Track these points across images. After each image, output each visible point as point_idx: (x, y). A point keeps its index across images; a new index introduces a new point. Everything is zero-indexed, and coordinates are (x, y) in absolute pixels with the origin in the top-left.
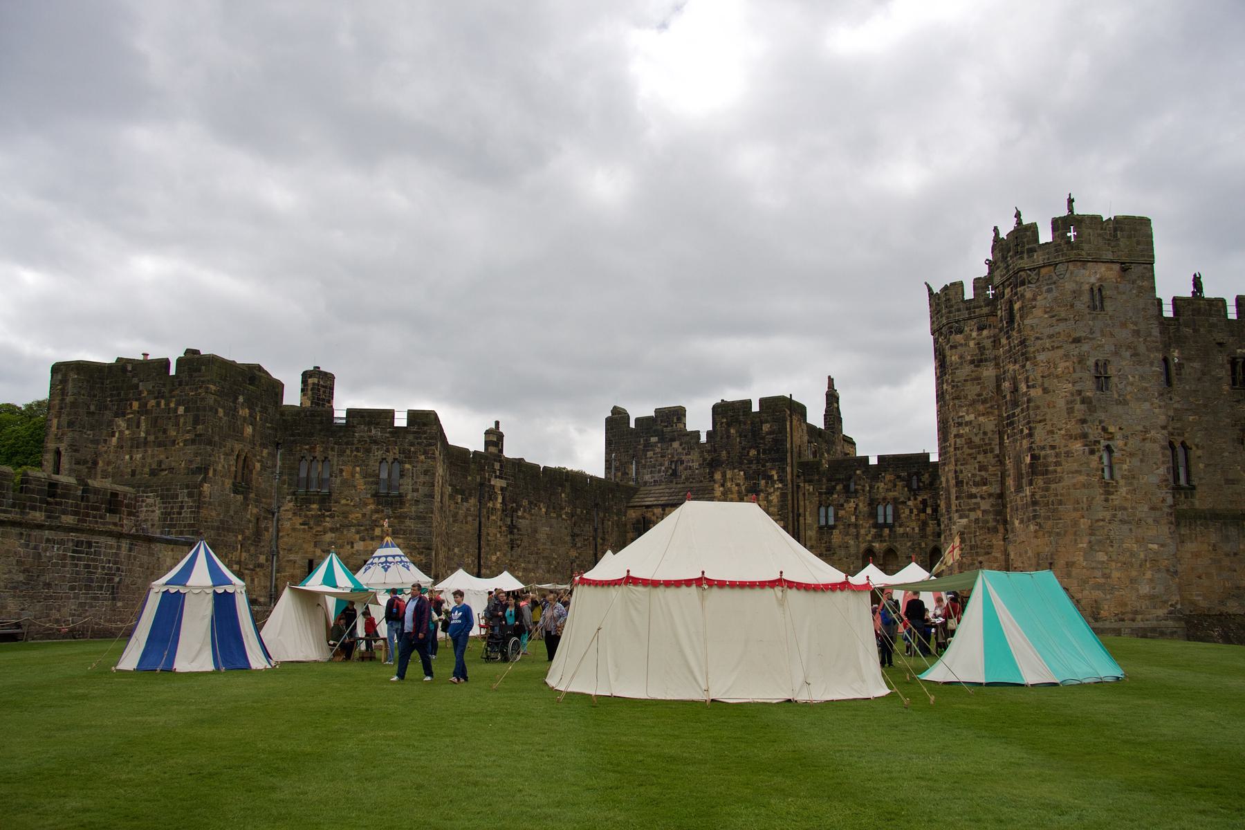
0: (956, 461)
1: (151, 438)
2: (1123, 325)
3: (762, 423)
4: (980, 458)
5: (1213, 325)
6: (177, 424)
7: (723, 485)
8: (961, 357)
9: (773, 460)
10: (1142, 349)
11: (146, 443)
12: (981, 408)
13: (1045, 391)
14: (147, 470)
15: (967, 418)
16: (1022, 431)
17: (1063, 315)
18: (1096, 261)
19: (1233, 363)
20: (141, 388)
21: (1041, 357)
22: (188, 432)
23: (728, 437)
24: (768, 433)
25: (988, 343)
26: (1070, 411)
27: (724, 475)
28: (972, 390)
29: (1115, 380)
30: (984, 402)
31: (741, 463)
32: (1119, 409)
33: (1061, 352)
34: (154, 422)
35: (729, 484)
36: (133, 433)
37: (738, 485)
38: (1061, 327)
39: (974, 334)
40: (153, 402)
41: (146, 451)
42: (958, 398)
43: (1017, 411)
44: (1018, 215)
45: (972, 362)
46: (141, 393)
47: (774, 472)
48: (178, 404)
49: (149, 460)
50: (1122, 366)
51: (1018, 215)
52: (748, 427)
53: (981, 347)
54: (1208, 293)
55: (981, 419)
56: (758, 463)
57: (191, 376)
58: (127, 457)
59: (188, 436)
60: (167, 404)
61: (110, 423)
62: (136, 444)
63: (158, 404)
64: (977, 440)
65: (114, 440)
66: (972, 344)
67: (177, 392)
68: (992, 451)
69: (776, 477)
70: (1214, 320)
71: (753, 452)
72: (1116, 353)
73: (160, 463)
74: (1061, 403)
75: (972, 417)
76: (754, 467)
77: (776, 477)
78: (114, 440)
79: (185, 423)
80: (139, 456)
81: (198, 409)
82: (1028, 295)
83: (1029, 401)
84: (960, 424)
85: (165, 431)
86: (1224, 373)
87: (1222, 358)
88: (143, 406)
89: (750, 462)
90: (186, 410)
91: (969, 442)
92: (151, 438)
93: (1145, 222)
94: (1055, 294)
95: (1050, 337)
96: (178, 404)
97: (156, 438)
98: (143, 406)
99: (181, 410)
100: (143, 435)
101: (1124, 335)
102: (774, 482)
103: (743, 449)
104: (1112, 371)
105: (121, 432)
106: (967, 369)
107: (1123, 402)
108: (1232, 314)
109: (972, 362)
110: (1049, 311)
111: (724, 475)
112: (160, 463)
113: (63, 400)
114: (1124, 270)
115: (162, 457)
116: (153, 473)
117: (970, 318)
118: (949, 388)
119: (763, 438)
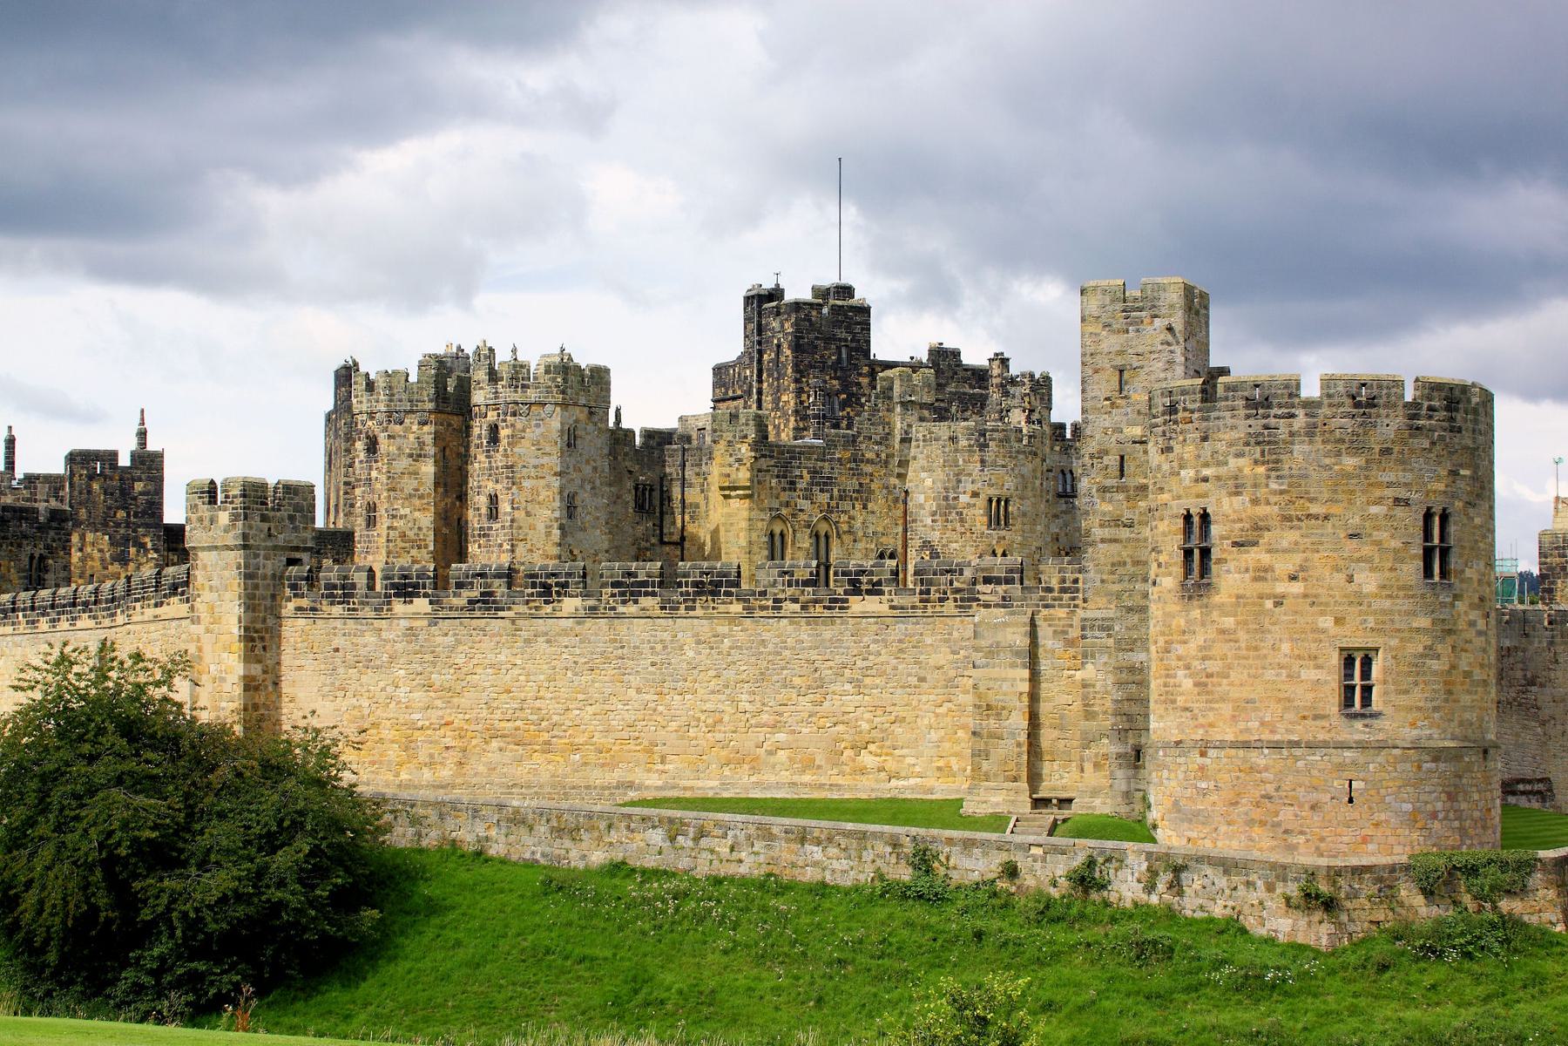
0: (389, 553)
2: (588, 462)
3: (134, 480)
4: (414, 552)
5: (626, 454)
7: (81, 550)
8: (399, 449)
9: (147, 526)
10: (598, 482)
12: (417, 502)
13: (528, 514)
15: (402, 512)
16: (501, 545)
17: (548, 449)
18: (575, 404)
19: (636, 489)
21: (526, 484)
23: (89, 492)
24: (141, 494)
25: (429, 439)
26: (548, 534)
27: (83, 537)
28: (409, 484)
29: (579, 509)
30: (421, 497)
31: (105, 525)
32: (580, 535)
33: (542, 482)
35: (89, 549)
37: (101, 551)
38: (545, 460)
39: (415, 428)
42: (393, 489)
43: (495, 526)
44: (514, 351)
45: (411, 456)
47: (147, 540)
50: (584, 496)
51: (514, 351)
52: (116, 483)
53: (422, 444)
54: (625, 425)
55: (417, 514)
56: (128, 526)
64: (411, 534)
66: (411, 437)
68: (426, 547)
69: (149, 545)
70: (627, 449)
71: (121, 514)
72: (582, 487)
74: (541, 527)
75: (407, 511)
76: (122, 531)
77: (149, 545)
82: (519, 426)
83: (512, 521)
84: (394, 517)
86: (629, 498)
87: (629, 484)
89: (118, 525)
91: (403, 535)
93: (607, 371)
94: (542, 429)
95: (535, 467)
101: (588, 470)
102: (146, 551)
103: (109, 508)
104: (578, 502)
106: (404, 463)
107: (583, 529)
108: (638, 441)
109: (411, 456)
110: (536, 443)
111: (83, 537)
114: (591, 413)
117: (412, 412)
118: (383, 478)
119: (135, 499)
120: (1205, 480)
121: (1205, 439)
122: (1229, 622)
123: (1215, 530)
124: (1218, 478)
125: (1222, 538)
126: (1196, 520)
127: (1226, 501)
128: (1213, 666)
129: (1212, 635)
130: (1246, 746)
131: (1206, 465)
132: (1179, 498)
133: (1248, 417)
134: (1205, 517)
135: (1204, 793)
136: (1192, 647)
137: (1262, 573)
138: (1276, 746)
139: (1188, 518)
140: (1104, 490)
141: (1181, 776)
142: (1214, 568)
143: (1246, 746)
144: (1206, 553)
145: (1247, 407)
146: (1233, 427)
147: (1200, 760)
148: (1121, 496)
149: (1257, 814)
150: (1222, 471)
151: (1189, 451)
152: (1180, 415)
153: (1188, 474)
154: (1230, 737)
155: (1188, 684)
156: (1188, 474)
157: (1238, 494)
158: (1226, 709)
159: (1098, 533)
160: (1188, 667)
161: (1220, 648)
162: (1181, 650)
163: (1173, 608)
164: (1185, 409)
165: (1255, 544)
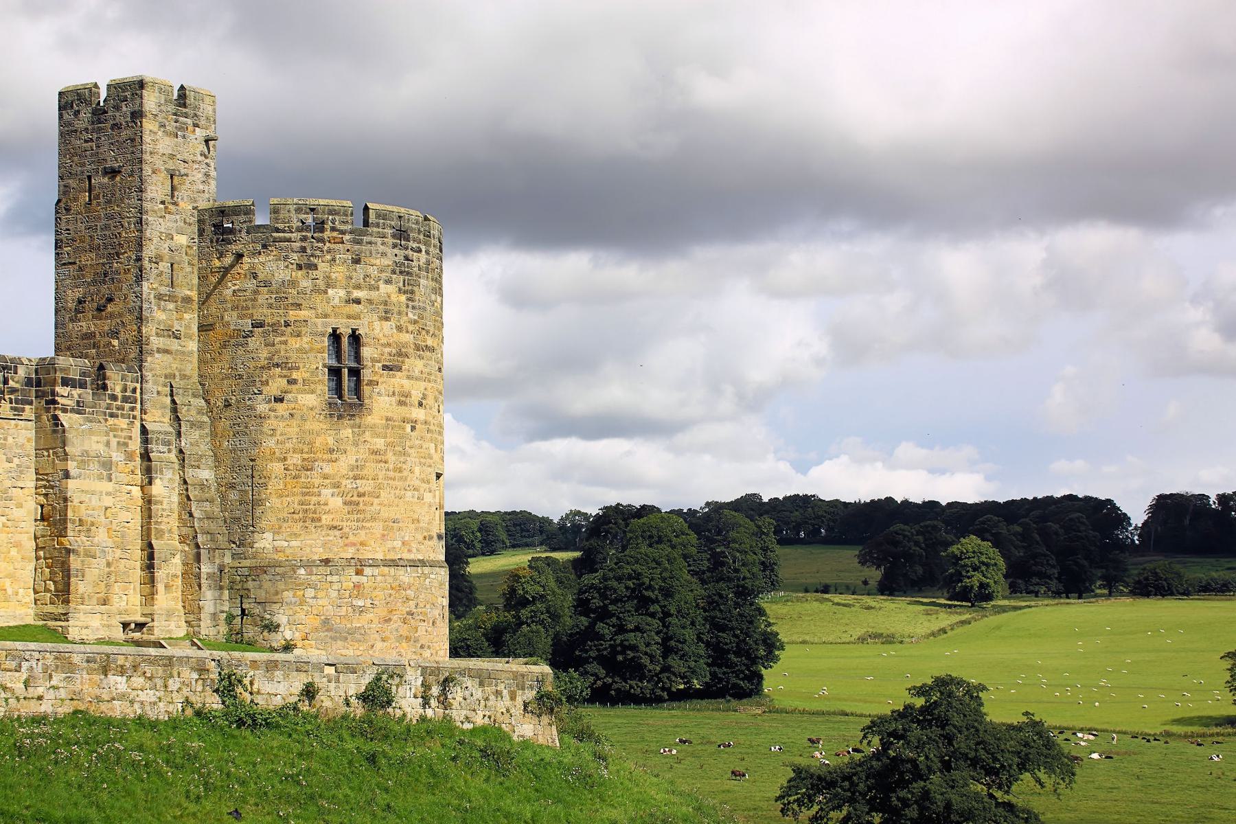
120: (358, 301)
121: (357, 261)
122: (379, 443)
123: (366, 352)
124: (370, 301)
125: (373, 360)
126: (345, 341)
127: (377, 324)
128: (365, 486)
129: (363, 452)
130: (393, 564)
131: (358, 287)
132: (326, 316)
133: (395, 246)
134: (355, 338)
135: (362, 611)
136: (344, 463)
137: (403, 399)
138: (414, 564)
139: (335, 337)
140: (159, 297)
141: (334, 594)
142: (366, 390)
143: (393, 564)
144: (355, 373)
145: (394, 236)
146: (384, 254)
147: (356, 579)
148: (171, 306)
149: (404, 630)
150: (374, 295)
151: (339, 272)
152: (327, 234)
153: (337, 294)
154: (380, 556)
155: (336, 502)
156: (337, 294)
157: (387, 319)
158: (378, 528)
159: (156, 342)
160: (337, 486)
161: (370, 468)
162: (328, 469)
163: (317, 424)
164: (333, 229)
165: (400, 369)
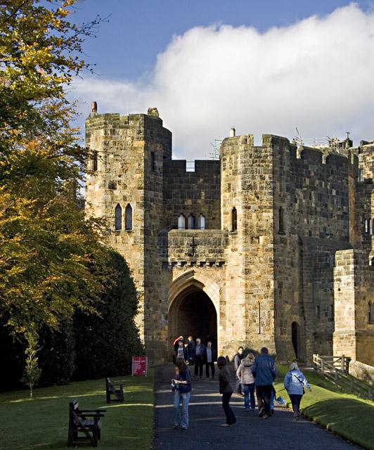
1: (319, 209)
6: (333, 202)
11: (316, 212)
14: (318, 233)
20: (310, 169)
22: (339, 209)
34: (320, 197)
36: (308, 203)
40: (317, 182)
41: (316, 219)
46: (310, 172)
48: (332, 187)
49: (318, 225)
57: (337, 168)
58: (305, 220)
59: (339, 213)
60: (326, 186)
61: (293, 193)
62: (311, 212)
63: (321, 185)
65: (297, 205)
67: (331, 178)
73: (325, 229)
78: (297, 205)
79: (337, 202)
80: (312, 221)
81: (343, 194)
85: (326, 206)
88: (312, 183)
90: (337, 193)
92: (319, 209)
96: (332, 187)
97: (322, 209)
98: (312, 183)
99: (334, 192)
100: (313, 205)
105: (301, 201)
112: (325, 229)
113: (282, 168)
115: (326, 225)
116: (322, 236)
